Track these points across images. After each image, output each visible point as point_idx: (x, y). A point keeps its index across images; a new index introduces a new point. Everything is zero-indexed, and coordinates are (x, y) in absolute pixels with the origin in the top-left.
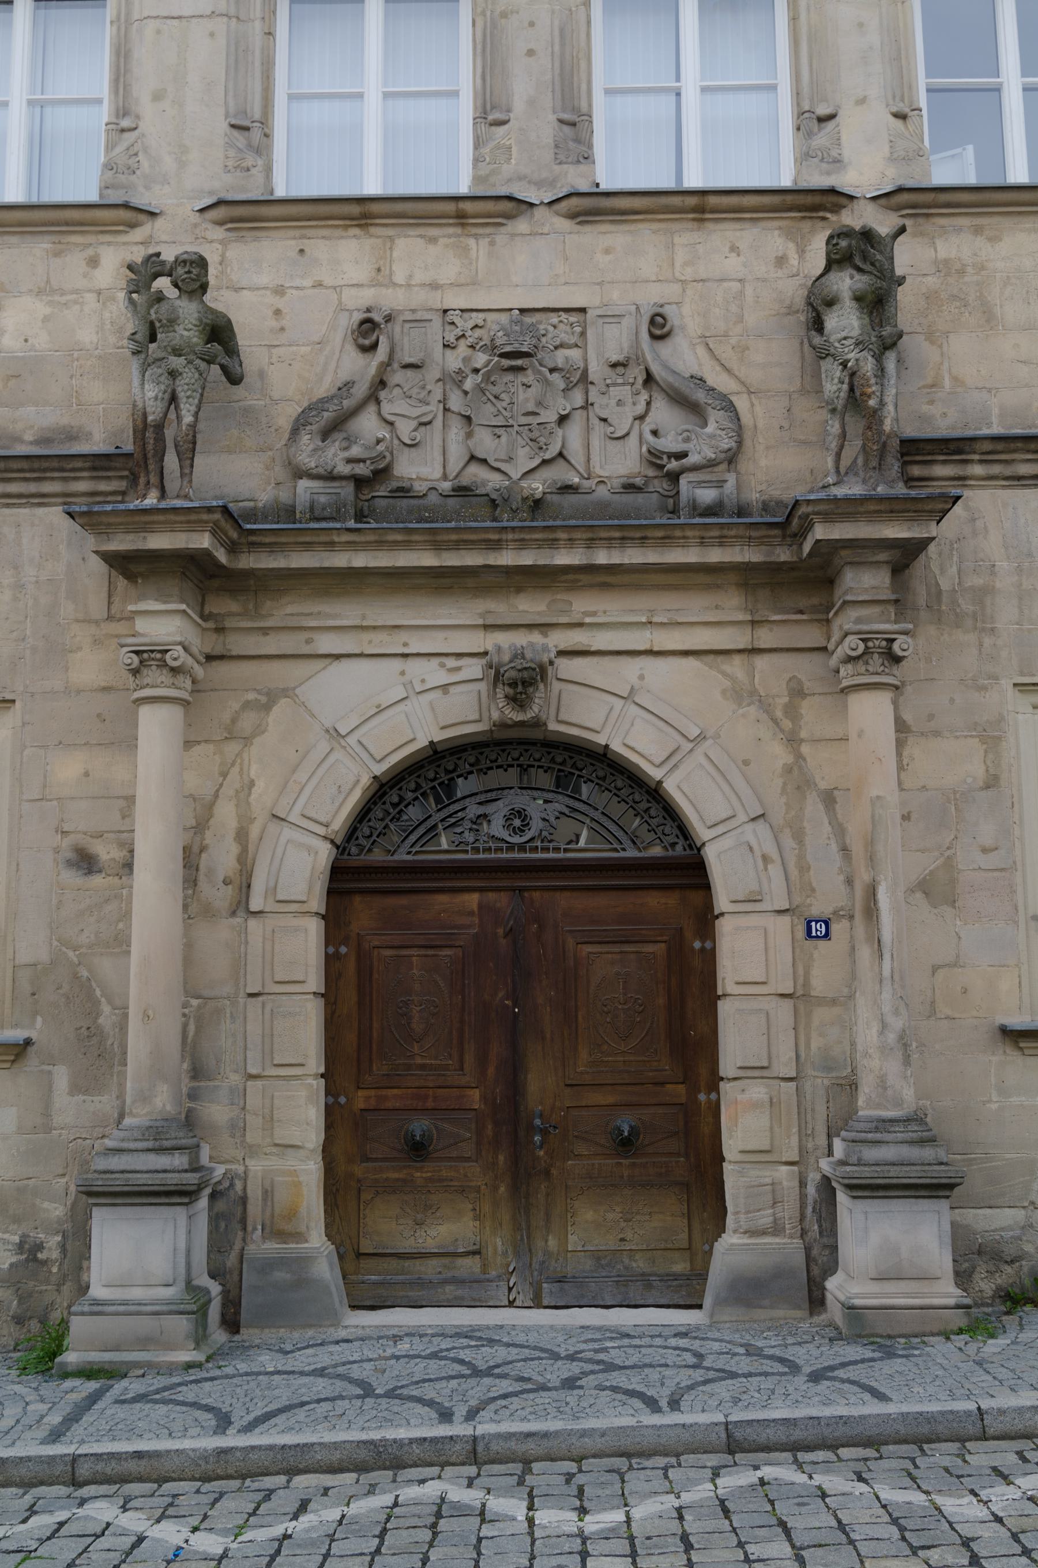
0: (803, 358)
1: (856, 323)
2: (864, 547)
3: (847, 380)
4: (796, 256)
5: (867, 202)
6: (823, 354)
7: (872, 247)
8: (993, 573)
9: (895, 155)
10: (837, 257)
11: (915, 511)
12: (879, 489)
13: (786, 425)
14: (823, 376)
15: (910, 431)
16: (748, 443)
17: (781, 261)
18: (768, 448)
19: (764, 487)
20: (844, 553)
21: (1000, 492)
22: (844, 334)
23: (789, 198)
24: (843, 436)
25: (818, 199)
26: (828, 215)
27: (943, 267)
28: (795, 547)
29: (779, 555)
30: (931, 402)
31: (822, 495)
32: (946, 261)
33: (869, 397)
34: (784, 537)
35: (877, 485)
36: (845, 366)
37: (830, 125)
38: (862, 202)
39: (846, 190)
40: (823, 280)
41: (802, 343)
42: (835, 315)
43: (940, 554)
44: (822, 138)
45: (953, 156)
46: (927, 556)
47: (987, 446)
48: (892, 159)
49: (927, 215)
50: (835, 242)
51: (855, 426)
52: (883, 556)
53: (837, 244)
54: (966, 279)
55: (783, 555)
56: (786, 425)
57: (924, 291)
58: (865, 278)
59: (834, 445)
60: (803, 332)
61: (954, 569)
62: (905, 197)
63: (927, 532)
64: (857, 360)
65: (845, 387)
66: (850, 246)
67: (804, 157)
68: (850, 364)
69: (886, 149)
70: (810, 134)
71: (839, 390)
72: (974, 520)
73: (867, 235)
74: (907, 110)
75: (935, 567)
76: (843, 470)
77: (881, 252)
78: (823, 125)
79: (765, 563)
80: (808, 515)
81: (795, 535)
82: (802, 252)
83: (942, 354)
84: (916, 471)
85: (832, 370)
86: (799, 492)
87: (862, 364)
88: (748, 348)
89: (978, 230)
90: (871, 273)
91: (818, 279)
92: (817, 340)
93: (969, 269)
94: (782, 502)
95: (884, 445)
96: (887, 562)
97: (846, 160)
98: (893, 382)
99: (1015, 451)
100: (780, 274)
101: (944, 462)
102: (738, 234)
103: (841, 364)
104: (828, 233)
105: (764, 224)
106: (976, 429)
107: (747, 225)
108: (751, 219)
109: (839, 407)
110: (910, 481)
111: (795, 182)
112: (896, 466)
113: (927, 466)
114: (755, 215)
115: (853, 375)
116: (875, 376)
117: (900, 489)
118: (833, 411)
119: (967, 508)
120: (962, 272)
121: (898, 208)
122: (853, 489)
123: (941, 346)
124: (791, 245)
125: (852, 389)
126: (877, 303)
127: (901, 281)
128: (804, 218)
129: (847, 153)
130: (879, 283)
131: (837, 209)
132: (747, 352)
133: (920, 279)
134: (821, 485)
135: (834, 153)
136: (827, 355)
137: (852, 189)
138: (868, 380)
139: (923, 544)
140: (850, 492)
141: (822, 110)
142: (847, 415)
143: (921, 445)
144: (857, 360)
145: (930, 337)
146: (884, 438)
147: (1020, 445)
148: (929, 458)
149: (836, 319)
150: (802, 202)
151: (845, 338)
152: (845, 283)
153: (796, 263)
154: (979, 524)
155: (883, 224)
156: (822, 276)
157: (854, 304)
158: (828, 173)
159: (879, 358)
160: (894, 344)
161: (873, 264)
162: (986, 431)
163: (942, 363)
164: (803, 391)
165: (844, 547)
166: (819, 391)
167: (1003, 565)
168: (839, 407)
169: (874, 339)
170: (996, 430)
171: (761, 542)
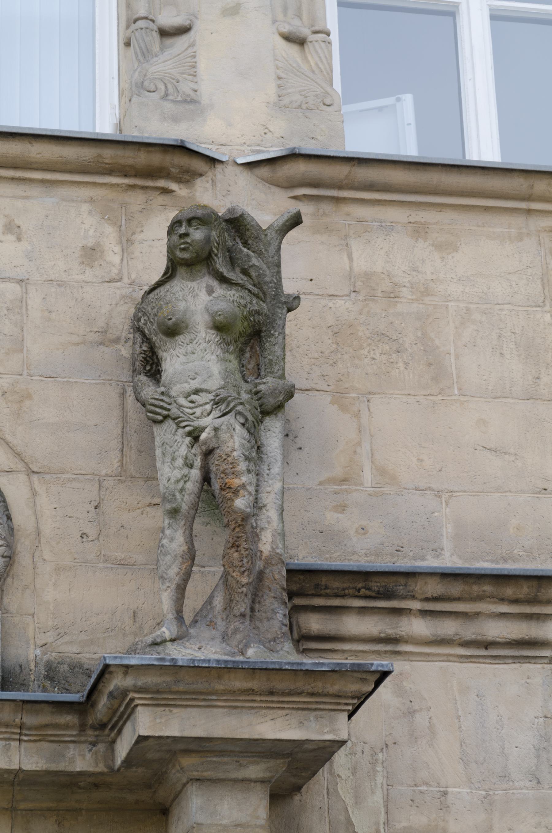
0: (124, 418)
1: (216, 368)
2: (221, 753)
3: (198, 462)
4: (118, 249)
5: (238, 170)
6: (159, 415)
7: (245, 244)
8: (444, 807)
9: (286, 101)
10: (186, 255)
11: (312, 694)
12: (250, 652)
13: (92, 533)
14: (158, 452)
15: (305, 556)
16: (23, 559)
17: (91, 254)
18: (58, 570)
19: (49, 638)
20: (187, 761)
21: (455, 667)
22: (194, 385)
23: (108, 153)
24: (191, 556)
25: (157, 159)
26: (173, 186)
27: (362, 286)
28: (101, 747)
29: (72, 761)
30: (341, 508)
31: (150, 658)
32: (368, 277)
33: (236, 492)
34: (83, 727)
35: (247, 646)
36: (196, 439)
37: (181, 42)
38: (230, 170)
39: (202, 149)
40: (162, 291)
41: (123, 394)
42: (180, 351)
43: (354, 770)
44: (167, 60)
45: (380, 109)
46: (331, 772)
47: (434, 588)
48: (280, 105)
49: (337, 200)
50: (182, 230)
51: (212, 540)
52: (255, 770)
53: (186, 235)
54: (400, 308)
55: (81, 760)
56: (92, 533)
57: (331, 321)
58: (232, 294)
59: (174, 572)
60: (125, 375)
61: (378, 797)
62: (300, 169)
63: (333, 731)
64: (216, 429)
65: (196, 473)
66: (208, 240)
67: (135, 89)
68: (203, 436)
69: (272, 89)
70: (146, 54)
71: (185, 478)
72: (411, 713)
73: (237, 224)
74: (305, 31)
75: (344, 791)
76: (188, 616)
77: (260, 254)
78: (169, 41)
79: (48, 773)
80: (124, 693)
81: (102, 726)
82: (127, 242)
83: (360, 429)
84: (314, 623)
85: (172, 443)
86: (111, 651)
87: (224, 436)
88: (29, 397)
89: (419, 231)
90: (242, 286)
91: (152, 290)
92: (150, 391)
93: (405, 292)
94: (81, 666)
95: (261, 576)
96: (262, 781)
97: (205, 100)
98: (276, 469)
99: (480, 598)
100: (89, 275)
101: (362, 610)
102: (19, 204)
103: (189, 434)
104: (172, 215)
105: (64, 191)
106: (415, 558)
107: (35, 191)
108: (43, 182)
109: (185, 507)
110: (303, 640)
111: (120, 127)
112: (281, 614)
113: (334, 612)
114: (49, 176)
115: (208, 453)
116: (247, 458)
117: (287, 655)
118: (174, 513)
119: (400, 692)
120: (392, 296)
121: (289, 185)
122: (205, 649)
123: (357, 415)
124: (109, 230)
125: (206, 479)
126: (251, 338)
127: (292, 303)
128: (132, 187)
129: (206, 90)
130: (255, 305)
131: (187, 177)
132: (27, 403)
133: (324, 302)
134: (149, 639)
135: (186, 87)
136: (166, 417)
137: (214, 147)
138: (234, 464)
139: (325, 752)
140: (200, 655)
141: (169, 18)
142: (197, 520)
143: (324, 580)
144: (216, 429)
145: (340, 397)
146: (260, 565)
147: (488, 588)
148: (337, 602)
149: (182, 359)
150: (130, 162)
151: (197, 392)
152: (198, 299)
153: (116, 259)
154: (421, 720)
155: (264, 208)
156: (159, 284)
157: (213, 335)
158: (175, 119)
159: (253, 429)
160: (280, 407)
161: (245, 272)
162: (431, 563)
163: (359, 444)
164: (123, 475)
165: (187, 752)
166: (150, 477)
167: (460, 793)
168: (185, 507)
169: (245, 396)
170: (450, 561)
171: (41, 735)
